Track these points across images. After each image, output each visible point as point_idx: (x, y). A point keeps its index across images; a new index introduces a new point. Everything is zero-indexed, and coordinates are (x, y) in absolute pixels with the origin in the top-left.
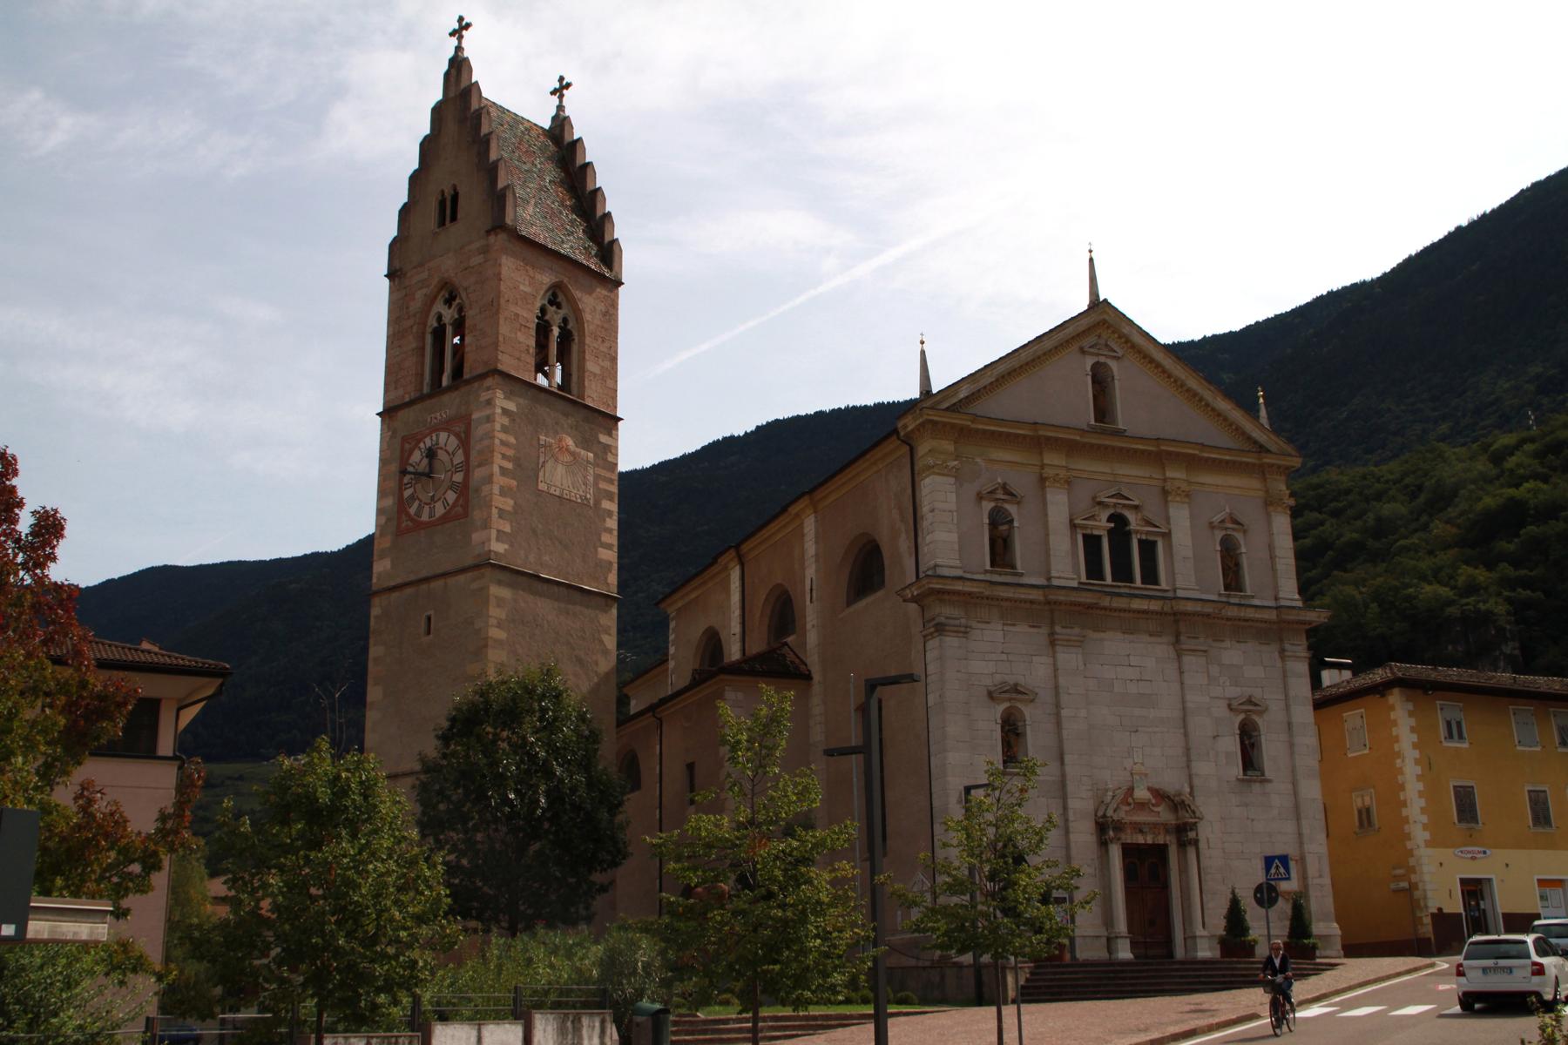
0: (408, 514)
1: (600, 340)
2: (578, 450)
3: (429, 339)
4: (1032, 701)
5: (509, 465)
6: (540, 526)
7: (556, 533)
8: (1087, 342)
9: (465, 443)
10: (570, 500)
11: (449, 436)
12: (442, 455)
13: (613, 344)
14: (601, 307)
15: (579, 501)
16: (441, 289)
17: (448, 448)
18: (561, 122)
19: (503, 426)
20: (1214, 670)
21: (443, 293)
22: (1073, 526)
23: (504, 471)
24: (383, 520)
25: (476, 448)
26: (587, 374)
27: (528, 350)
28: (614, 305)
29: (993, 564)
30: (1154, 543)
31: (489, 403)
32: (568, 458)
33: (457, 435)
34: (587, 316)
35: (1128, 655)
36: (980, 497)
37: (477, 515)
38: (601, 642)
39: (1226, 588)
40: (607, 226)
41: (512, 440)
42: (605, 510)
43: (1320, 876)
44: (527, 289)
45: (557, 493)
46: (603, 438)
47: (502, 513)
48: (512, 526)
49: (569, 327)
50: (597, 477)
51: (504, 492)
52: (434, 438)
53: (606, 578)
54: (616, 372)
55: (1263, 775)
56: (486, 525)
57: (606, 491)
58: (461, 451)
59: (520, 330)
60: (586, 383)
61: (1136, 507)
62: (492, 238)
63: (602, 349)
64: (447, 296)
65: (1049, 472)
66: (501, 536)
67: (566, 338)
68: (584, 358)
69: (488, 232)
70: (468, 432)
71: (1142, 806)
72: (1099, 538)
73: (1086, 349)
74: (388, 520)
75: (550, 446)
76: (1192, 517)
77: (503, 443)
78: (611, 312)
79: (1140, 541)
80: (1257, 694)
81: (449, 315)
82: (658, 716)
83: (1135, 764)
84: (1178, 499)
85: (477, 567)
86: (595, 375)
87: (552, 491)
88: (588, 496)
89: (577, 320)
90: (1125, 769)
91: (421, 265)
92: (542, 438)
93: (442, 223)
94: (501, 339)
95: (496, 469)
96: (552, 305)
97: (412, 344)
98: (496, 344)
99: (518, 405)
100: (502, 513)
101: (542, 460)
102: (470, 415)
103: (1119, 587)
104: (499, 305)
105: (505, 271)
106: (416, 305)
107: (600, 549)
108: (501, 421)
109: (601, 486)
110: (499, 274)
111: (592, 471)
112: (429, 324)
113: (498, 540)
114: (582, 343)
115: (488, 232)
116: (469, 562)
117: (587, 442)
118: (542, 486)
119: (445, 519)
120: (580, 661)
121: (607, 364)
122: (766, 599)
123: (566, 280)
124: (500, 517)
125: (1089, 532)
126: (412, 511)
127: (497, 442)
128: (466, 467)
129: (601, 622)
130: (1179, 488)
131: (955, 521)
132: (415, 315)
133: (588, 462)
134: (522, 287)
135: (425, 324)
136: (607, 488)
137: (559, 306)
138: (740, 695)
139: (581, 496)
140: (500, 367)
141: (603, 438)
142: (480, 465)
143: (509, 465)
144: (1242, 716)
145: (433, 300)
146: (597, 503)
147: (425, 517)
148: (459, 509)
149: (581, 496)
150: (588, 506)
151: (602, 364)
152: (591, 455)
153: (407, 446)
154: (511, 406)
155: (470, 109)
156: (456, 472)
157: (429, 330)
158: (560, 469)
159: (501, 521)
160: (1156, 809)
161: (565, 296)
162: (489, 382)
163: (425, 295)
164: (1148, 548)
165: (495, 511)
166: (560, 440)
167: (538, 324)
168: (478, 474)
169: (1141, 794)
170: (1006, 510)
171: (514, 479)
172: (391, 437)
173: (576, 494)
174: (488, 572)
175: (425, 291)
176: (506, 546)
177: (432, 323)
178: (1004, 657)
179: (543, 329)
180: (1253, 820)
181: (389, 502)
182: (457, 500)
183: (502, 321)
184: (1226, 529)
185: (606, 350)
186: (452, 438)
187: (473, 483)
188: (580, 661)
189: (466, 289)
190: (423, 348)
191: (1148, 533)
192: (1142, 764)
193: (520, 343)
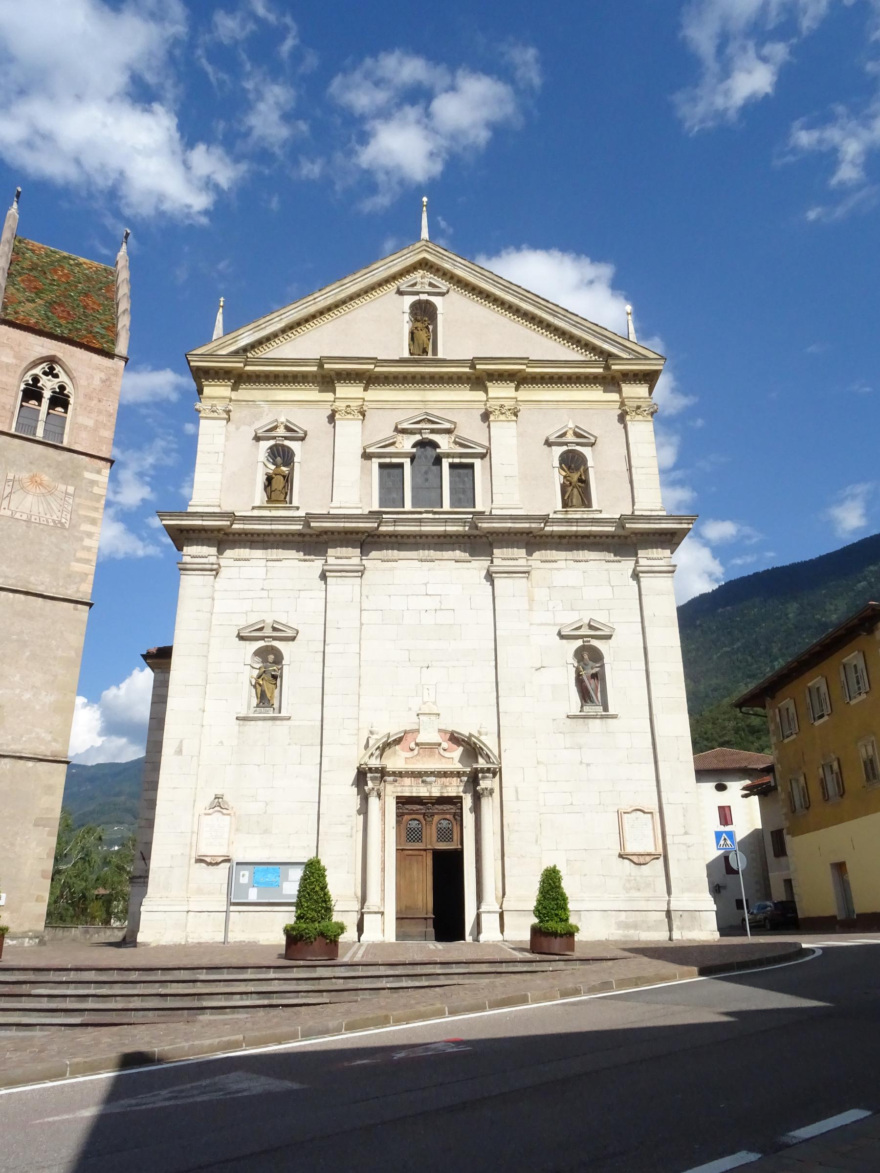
4: (293, 639)
8: (403, 283)
20: (541, 594)
22: (366, 456)
29: (270, 500)
30: (471, 466)
35: (426, 584)
36: (257, 439)
39: (565, 504)
43: (686, 833)
45: (24, 517)
46: (88, 475)
55: (606, 709)
57: (86, 517)
61: (449, 431)
65: (340, 405)
67: (60, 400)
71: (431, 747)
72: (401, 466)
73: (403, 288)
76: (520, 435)
79: (452, 466)
80: (600, 618)
83: (424, 703)
84: (502, 417)
87: (17, 516)
88: (63, 520)
90: (410, 709)
103: (420, 513)
107: (73, 564)
125: (387, 460)
130: (502, 406)
131: (220, 462)
133: (66, 493)
136: (88, 514)
137: (56, 376)
139: (54, 521)
141: (88, 475)
144: (579, 643)
149: (54, 521)
160: (446, 754)
164: (462, 470)
169: (429, 735)
170: (289, 448)
178: (264, 594)
179: (32, 393)
180: (588, 765)
184: (566, 444)
191: (461, 455)
192: (435, 703)
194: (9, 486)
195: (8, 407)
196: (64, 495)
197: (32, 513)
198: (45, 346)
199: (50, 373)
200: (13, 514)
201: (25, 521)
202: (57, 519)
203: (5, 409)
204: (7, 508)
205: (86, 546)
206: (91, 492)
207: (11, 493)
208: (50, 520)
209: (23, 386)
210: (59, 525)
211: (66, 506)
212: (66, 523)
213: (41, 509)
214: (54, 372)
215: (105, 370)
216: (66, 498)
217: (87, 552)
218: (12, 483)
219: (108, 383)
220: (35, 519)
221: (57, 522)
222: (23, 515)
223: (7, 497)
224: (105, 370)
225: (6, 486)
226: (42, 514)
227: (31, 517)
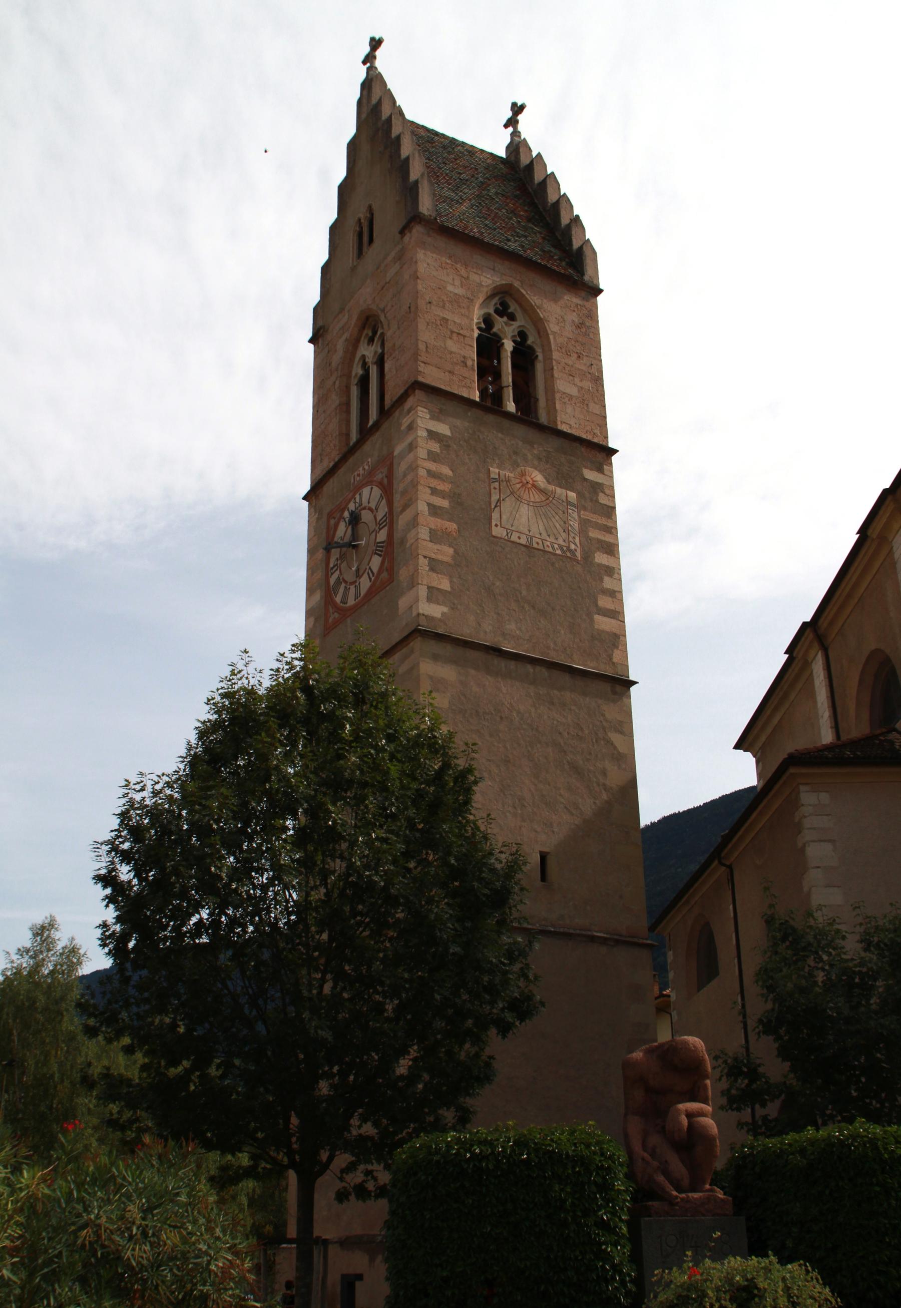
0: (335, 604)
1: (575, 356)
2: (551, 487)
3: (355, 391)
5: (445, 503)
6: (498, 583)
7: (524, 593)
9: (387, 491)
10: (544, 551)
11: (372, 488)
12: (366, 516)
13: (594, 362)
14: (573, 317)
15: (559, 552)
16: (364, 328)
17: (370, 505)
18: (517, 146)
19: (430, 452)
21: (365, 332)
23: (434, 510)
24: (311, 625)
25: (399, 487)
26: (557, 396)
27: (465, 364)
28: (592, 315)
31: (411, 427)
32: (536, 497)
33: (380, 485)
34: (552, 327)
37: (403, 574)
38: (609, 743)
40: (574, 231)
41: (446, 471)
42: (600, 565)
44: (460, 291)
45: (523, 541)
46: (590, 475)
47: (434, 565)
48: (451, 582)
49: (529, 342)
50: (585, 524)
51: (435, 536)
52: (358, 500)
53: (610, 657)
54: (603, 395)
56: (413, 583)
57: (600, 541)
58: (384, 501)
59: (450, 338)
60: (558, 406)
62: (406, 238)
63: (577, 366)
64: (370, 334)
66: (434, 594)
68: (552, 376)
69: (402, 232)
70: (390, 476)
74: (316, 620)
75: (508, 481)
77: (431, 474)
78: (588, 323)
81: (368, 351)
82: (728, 863)
85: (405, 641)
86: (571, 397)
87: (514, 538)
88: (573, 547)
89: (539, 333)
91: (342, 310)
92: (494, 471)
93: (360, 253)
94: (422, 346)
95: (422, 507)
96: (501, 316)
97: (335, 400)
98: (416, 355)
99: (453, 428)
100: (434, 565)
101: (495, 498)
102: (393, 452)
104: (417, 307)
105: (422, 268)
106: (337, 358)
107: (596, 617)
108: (425, 447)
109: (591, 534)
110: (416, 272)
111: (575, 515)
112: (353, 374)
113: (429, 599)
114: (548, 359)
115: (402, 232)
116: (396, 637)
117: (566, 479)
118: (497, 531)
119: (371, 593)
120: (576, 770)
121: (587, 384)
122: (861, 682)
123: (517, 284)
124: (432, 569)
126: (338, 599)
127: (422, 472)
128: (390, 520)
129: (608, 716)
132: (337, 370)
133: (569, 503)
134: (450, 288)
135: (349, 376)
136: (602, 538)
137: (512, 317)
138: (824, 797)
139: (561, 547)
140: (420, 379)
141: (590, 475)
142: (405, 508)
143: (445, 503)
145: (356, 343)
146: (587, 557)
147: (351, 602)
148: (385, 575)
149: (561, 547)
150: (573, 559)
151: (579, 384)
152: (572, 495)
153: (332, 522)
154: (443, 429)
155: (380, 118)
156: (380, 529)
157: (354, 381)
158: (525, 511)
159: (434, 575)
161: (520, 305)
162: (410, 402)
163: (346, 340)
165: (423, 562)
166: (523, 474)
167: (479, 335)
168: (402, 521)
171: (450, 520)
172: (318, 519)
173: (554, 543)
174: (417, 644)
175: (346, 335)
176: (445, 609)
177: (358, 371)
181: (318, 596)
182: (383, 563)
183: (421, 326)
185: (583, 368)
186: (375, 488)
187: (397, 536)
188: (576, 770)
189: (383, 310)
190: (348, 404)
193: (451, 353)
194: (495, 488)
195: (469, 363)
196: (565, 504)
197: (531, 534)
198: (496, 269)
199: (503, 311)
200: (509, 535)
201: (525, 546)
202: (563, 544)
203: (466, 366)
204: (499, 523)
205: (608, 590)
206: (597, 501)
207: (499, 500)
208: (556, 546)
209: (476, 333)
210: (568, 554)
211: (572, 523)
212: (576, 550)
213: (542, 528)
214: (509, 311)
215: (576, 309)
216: (570, 511)
217: (610, 599)
218: (497, 484)
219: (583, 330)
220: (538, 543)
221: (565, 548)
222: (522, 536)
223: (496, 506)
224: (576, 309)
225: (493, 490)
226: (544, 536)
227: (531, 539)
